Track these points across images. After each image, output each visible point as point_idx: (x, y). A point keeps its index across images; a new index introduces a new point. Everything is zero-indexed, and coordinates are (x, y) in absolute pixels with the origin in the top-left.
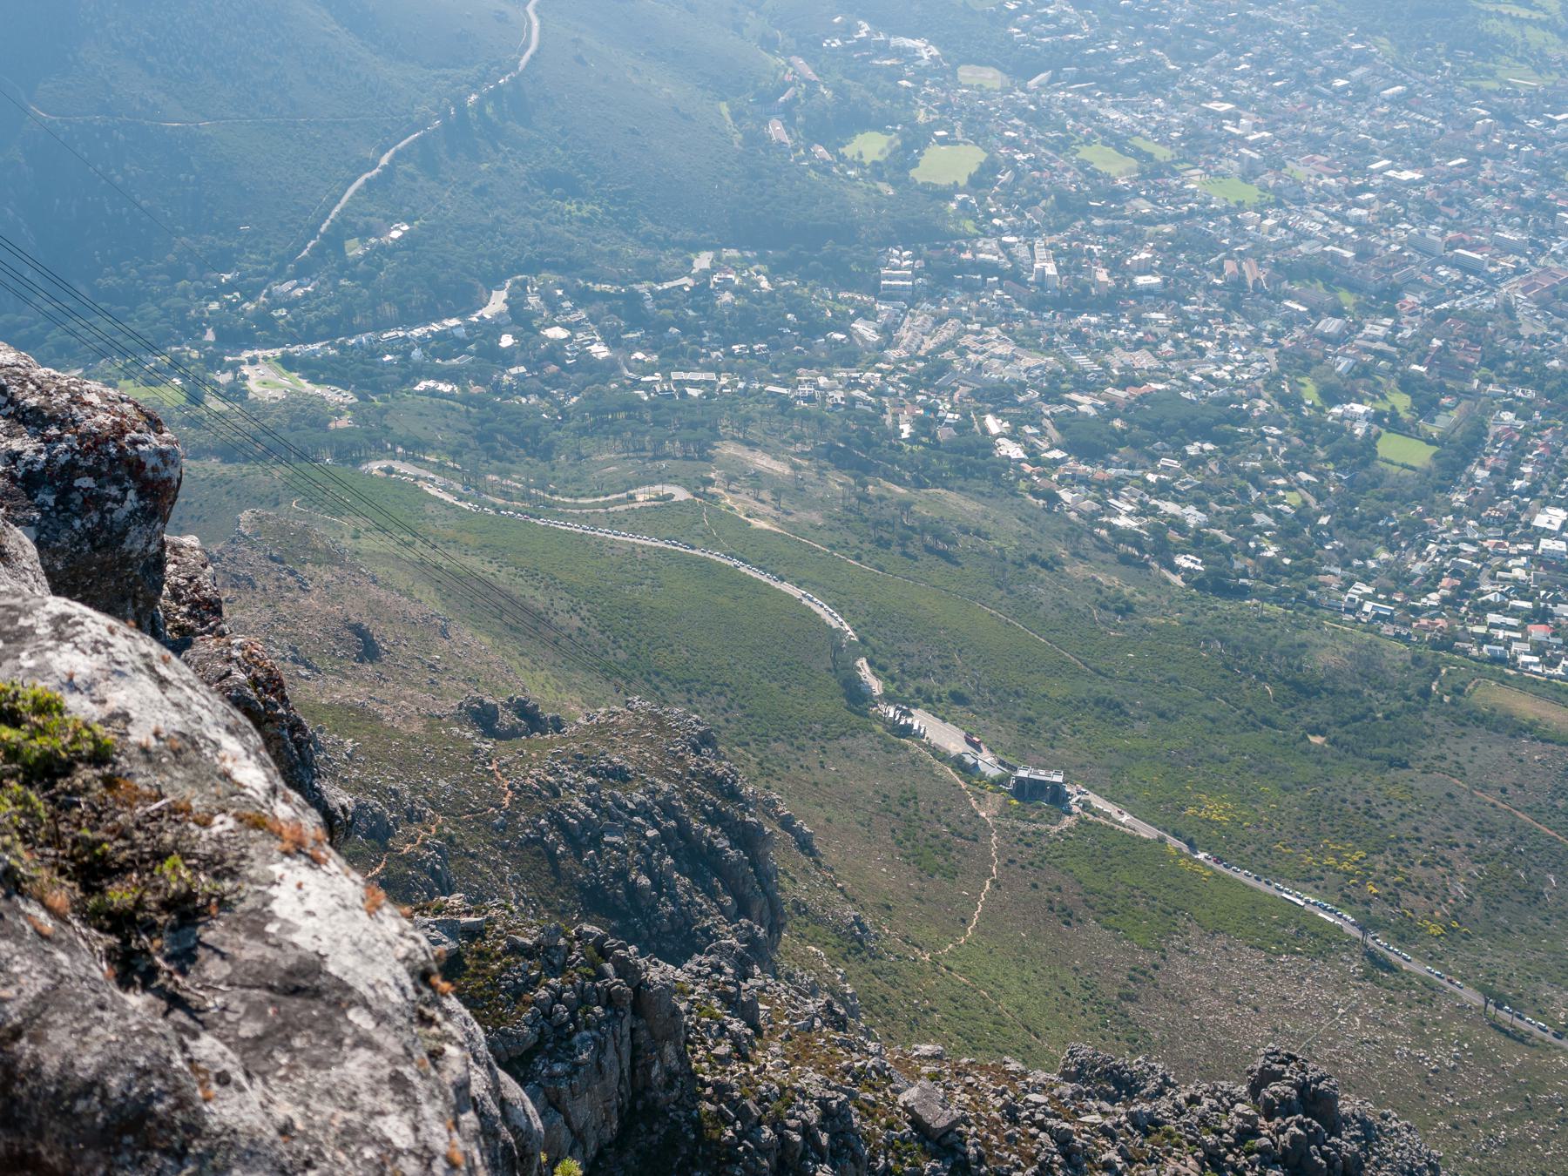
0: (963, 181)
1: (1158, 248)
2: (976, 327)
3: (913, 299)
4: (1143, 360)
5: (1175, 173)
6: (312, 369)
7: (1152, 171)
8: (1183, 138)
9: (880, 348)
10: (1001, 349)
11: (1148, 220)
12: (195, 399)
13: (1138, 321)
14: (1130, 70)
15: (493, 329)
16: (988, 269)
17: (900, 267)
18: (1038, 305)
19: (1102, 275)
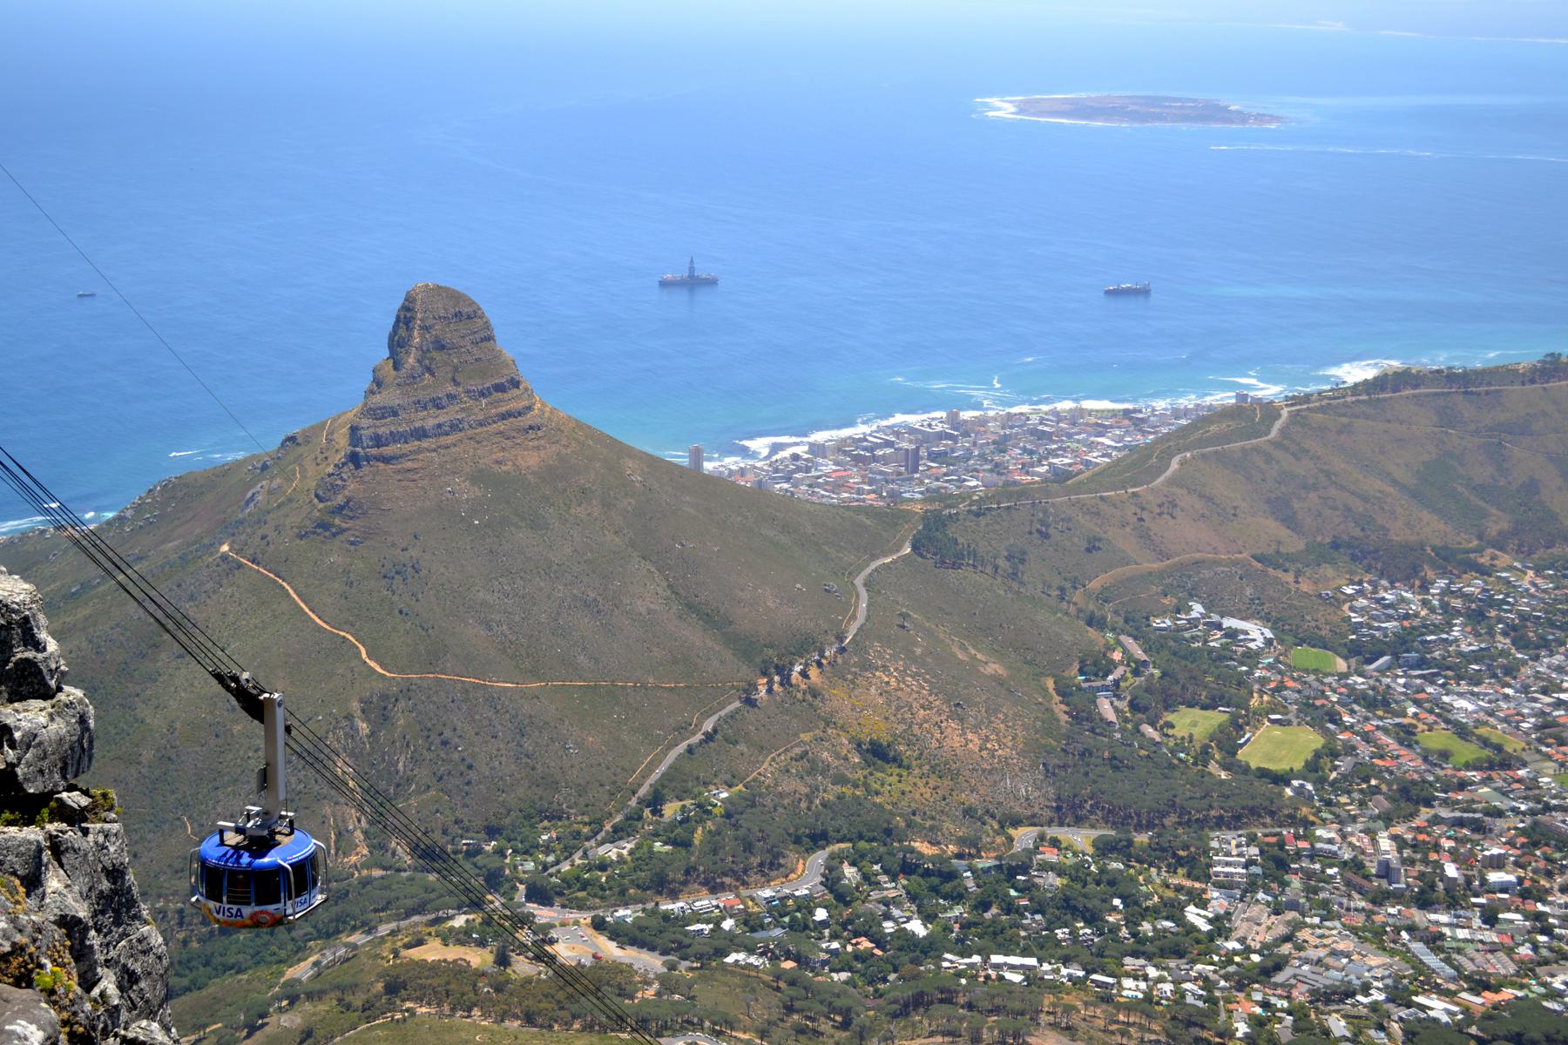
0: (1298, 765)
1: (1511, 843)
2: (1317, 920)
3: (1251, 886)
4: (1501, 966)
5: (1525, 765)
6: (618, 934)
7: (1499, 761)
8: (1537, 728)
9: (1211, 936)
10: (1341, 946)
11: (1500, 814)
12: (503, 960)
13: (1490, 919)
14: (1476, 657)
15: (807, 905)
16: (1330, 858)
17: (1232, 853)
18: (1380, 899)
19: (1451, 870)
